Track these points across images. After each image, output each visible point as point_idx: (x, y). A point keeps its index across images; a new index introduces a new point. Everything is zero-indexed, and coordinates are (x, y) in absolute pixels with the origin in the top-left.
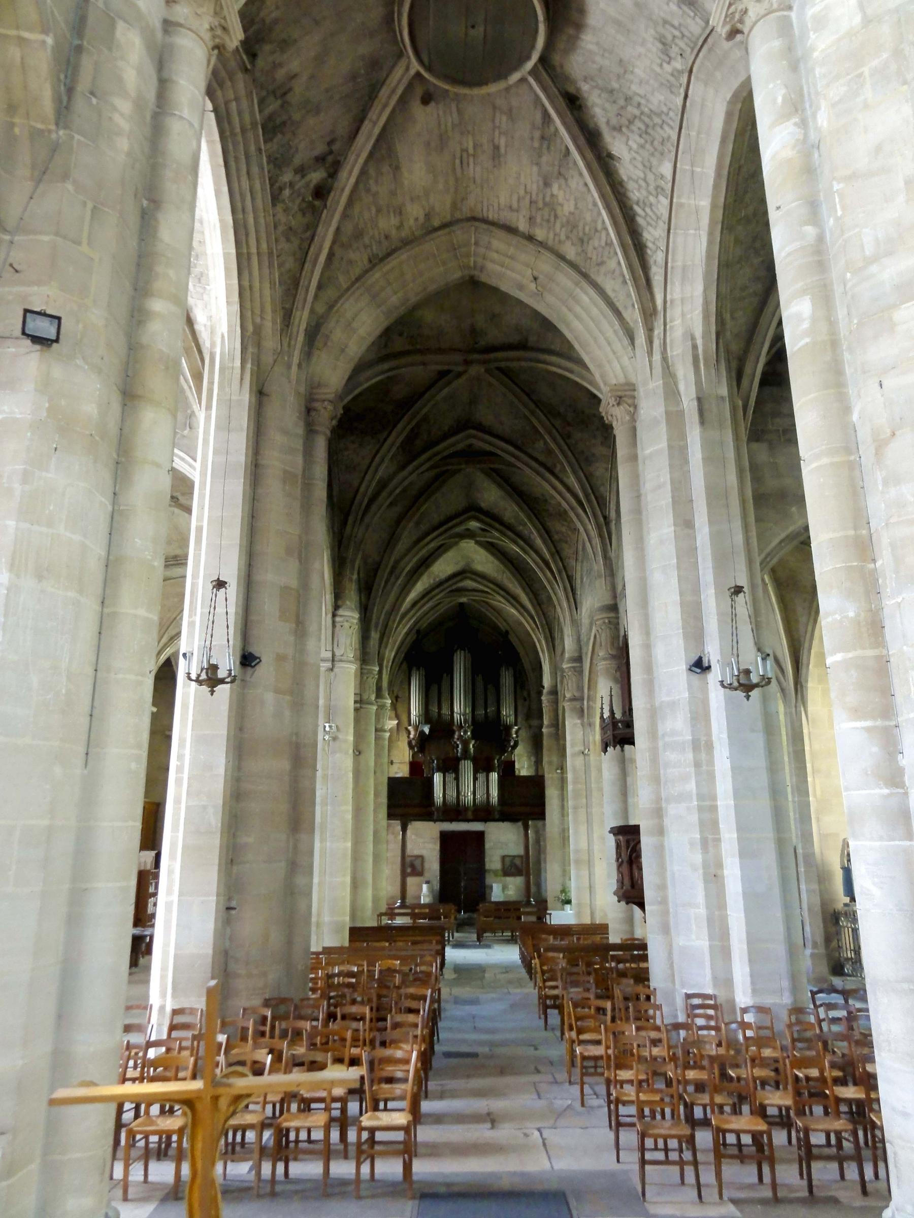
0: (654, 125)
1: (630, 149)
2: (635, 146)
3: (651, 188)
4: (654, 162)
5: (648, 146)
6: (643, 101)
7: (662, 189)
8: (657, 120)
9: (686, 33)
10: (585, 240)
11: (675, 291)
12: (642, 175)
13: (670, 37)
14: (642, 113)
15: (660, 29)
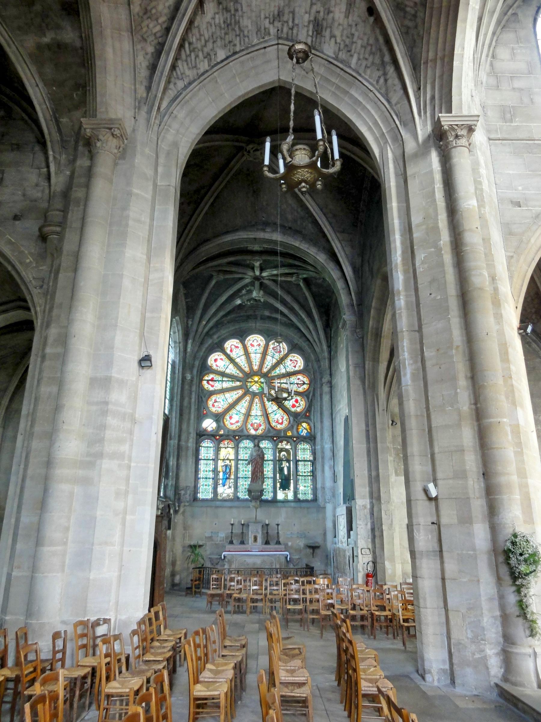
0: (233, 30)
1: (214, 18)
2: (217, 21)
3: (206, 50)
4: (219, 43)
5: (223, 32)
6: (240, 13)
7: (211, 59)
8: (237, 28)
9: (295, 31)
10: (148, 14)
11: (180, 113)
12: (207, 36)
13: (285, 18)
14: (234, 15)
15: (287, 11)
